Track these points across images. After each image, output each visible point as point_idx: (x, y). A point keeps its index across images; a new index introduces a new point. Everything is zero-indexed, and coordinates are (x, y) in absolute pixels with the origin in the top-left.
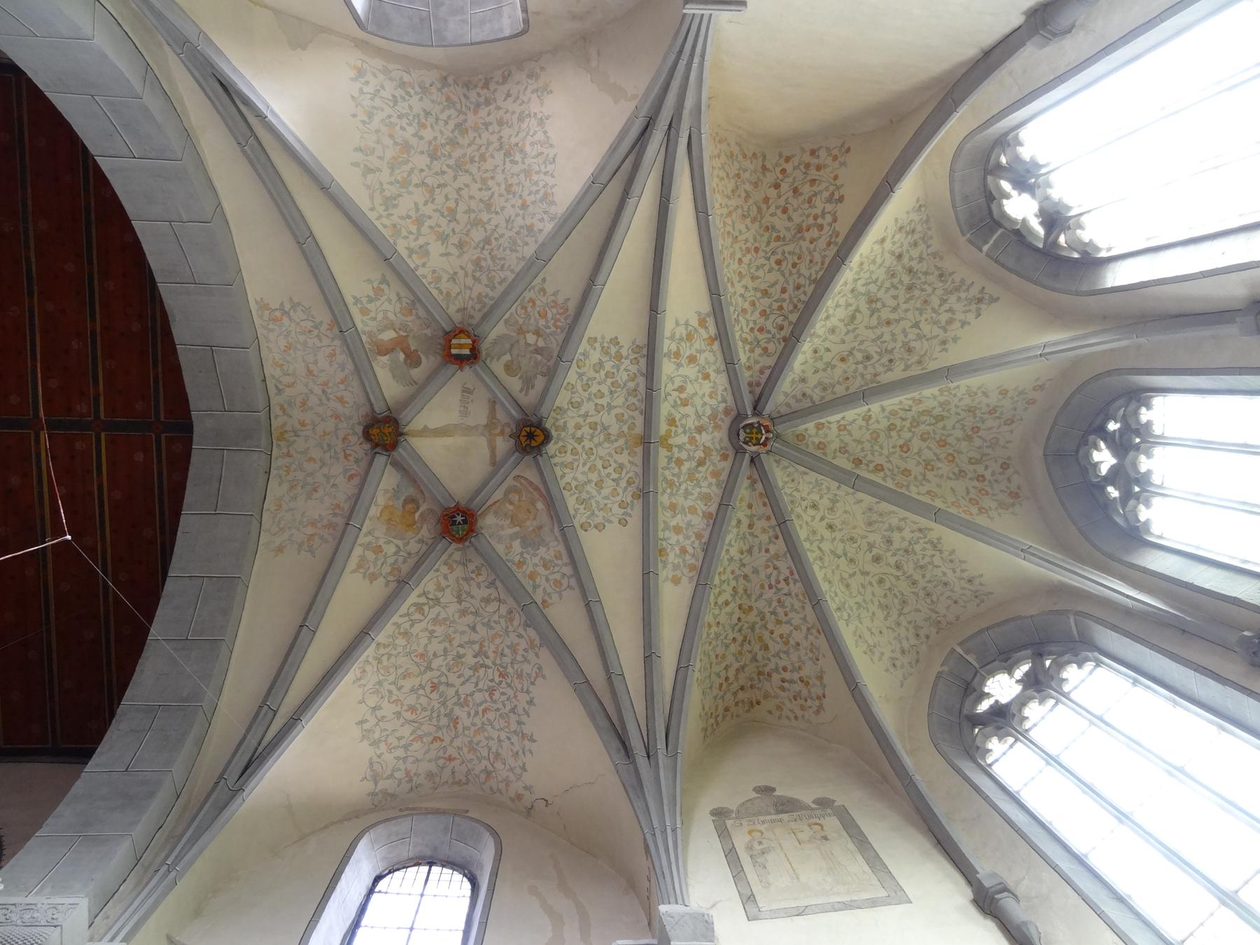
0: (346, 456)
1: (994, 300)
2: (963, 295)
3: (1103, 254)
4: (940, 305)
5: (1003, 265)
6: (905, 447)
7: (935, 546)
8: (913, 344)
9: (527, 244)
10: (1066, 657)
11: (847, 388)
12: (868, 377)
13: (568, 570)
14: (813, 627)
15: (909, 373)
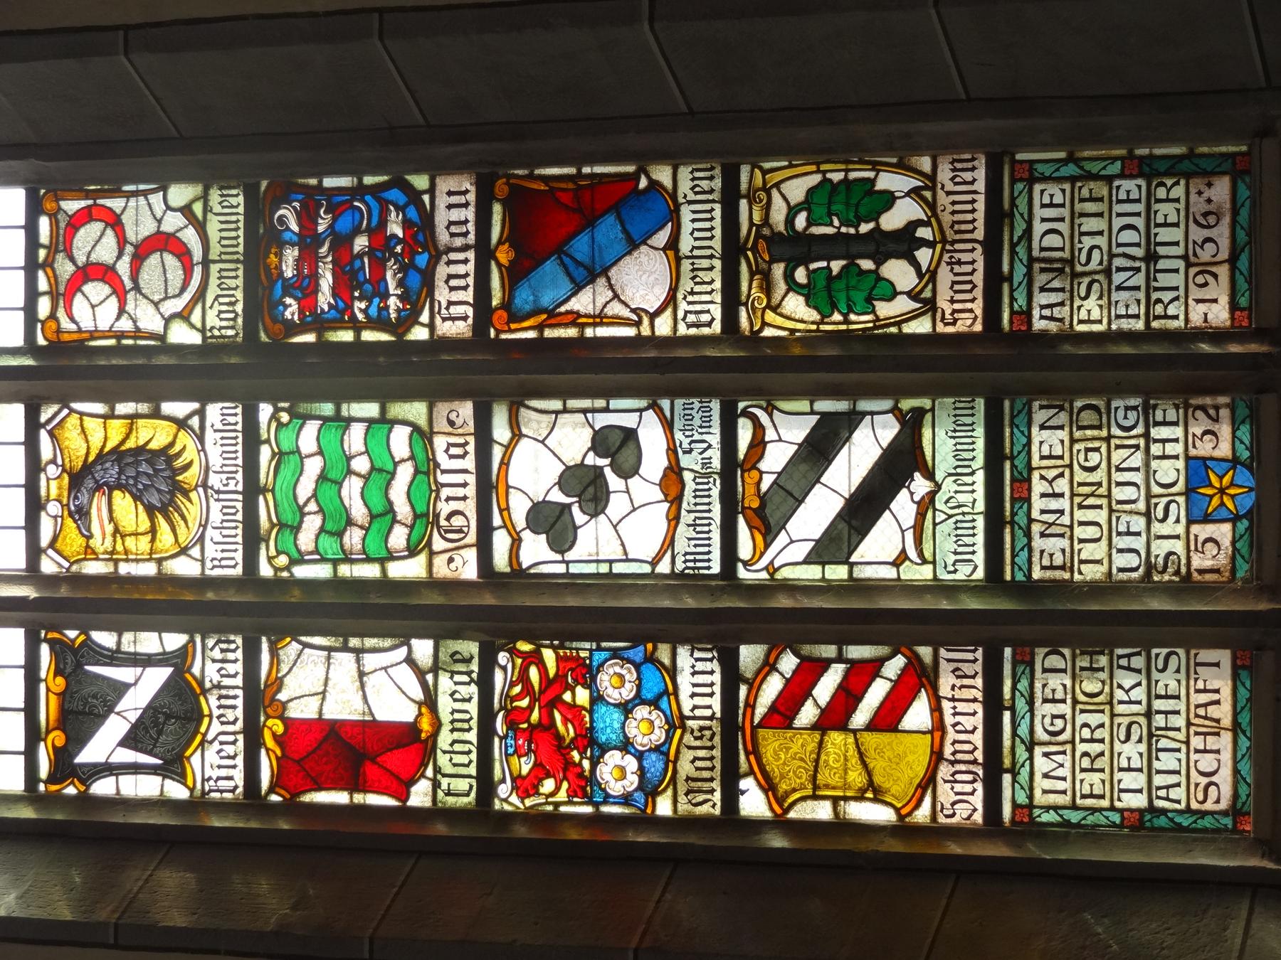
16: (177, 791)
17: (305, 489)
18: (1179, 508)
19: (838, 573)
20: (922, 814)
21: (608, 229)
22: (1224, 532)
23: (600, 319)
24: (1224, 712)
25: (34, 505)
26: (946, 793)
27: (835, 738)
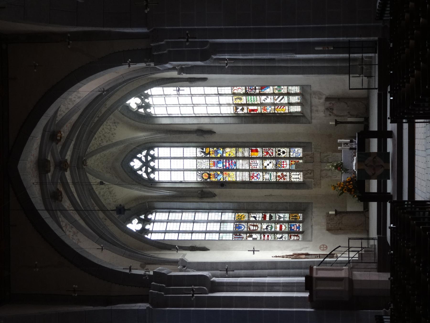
1: (118, 123)
2: (111, 121)
3: (154, 116)
4: (107, 124)
5: (123, 114)
6: (98, 165)
7: (110, 193)
8: (105, 135)
9: (69, 104)
10: (148, 213)
11: (94, 148)
12: (98, 144)
15: (108, 143)
16: (243, 112)
17: (249, 99)
18: (297, 99)
19: (280, 102)
20: (285, 112)
21: (266, 88)
22: (300, 100)
23: (266, 92)
24: (300, 107)
25: (233, 100)
26: (286, 111)
27: (280, 109)
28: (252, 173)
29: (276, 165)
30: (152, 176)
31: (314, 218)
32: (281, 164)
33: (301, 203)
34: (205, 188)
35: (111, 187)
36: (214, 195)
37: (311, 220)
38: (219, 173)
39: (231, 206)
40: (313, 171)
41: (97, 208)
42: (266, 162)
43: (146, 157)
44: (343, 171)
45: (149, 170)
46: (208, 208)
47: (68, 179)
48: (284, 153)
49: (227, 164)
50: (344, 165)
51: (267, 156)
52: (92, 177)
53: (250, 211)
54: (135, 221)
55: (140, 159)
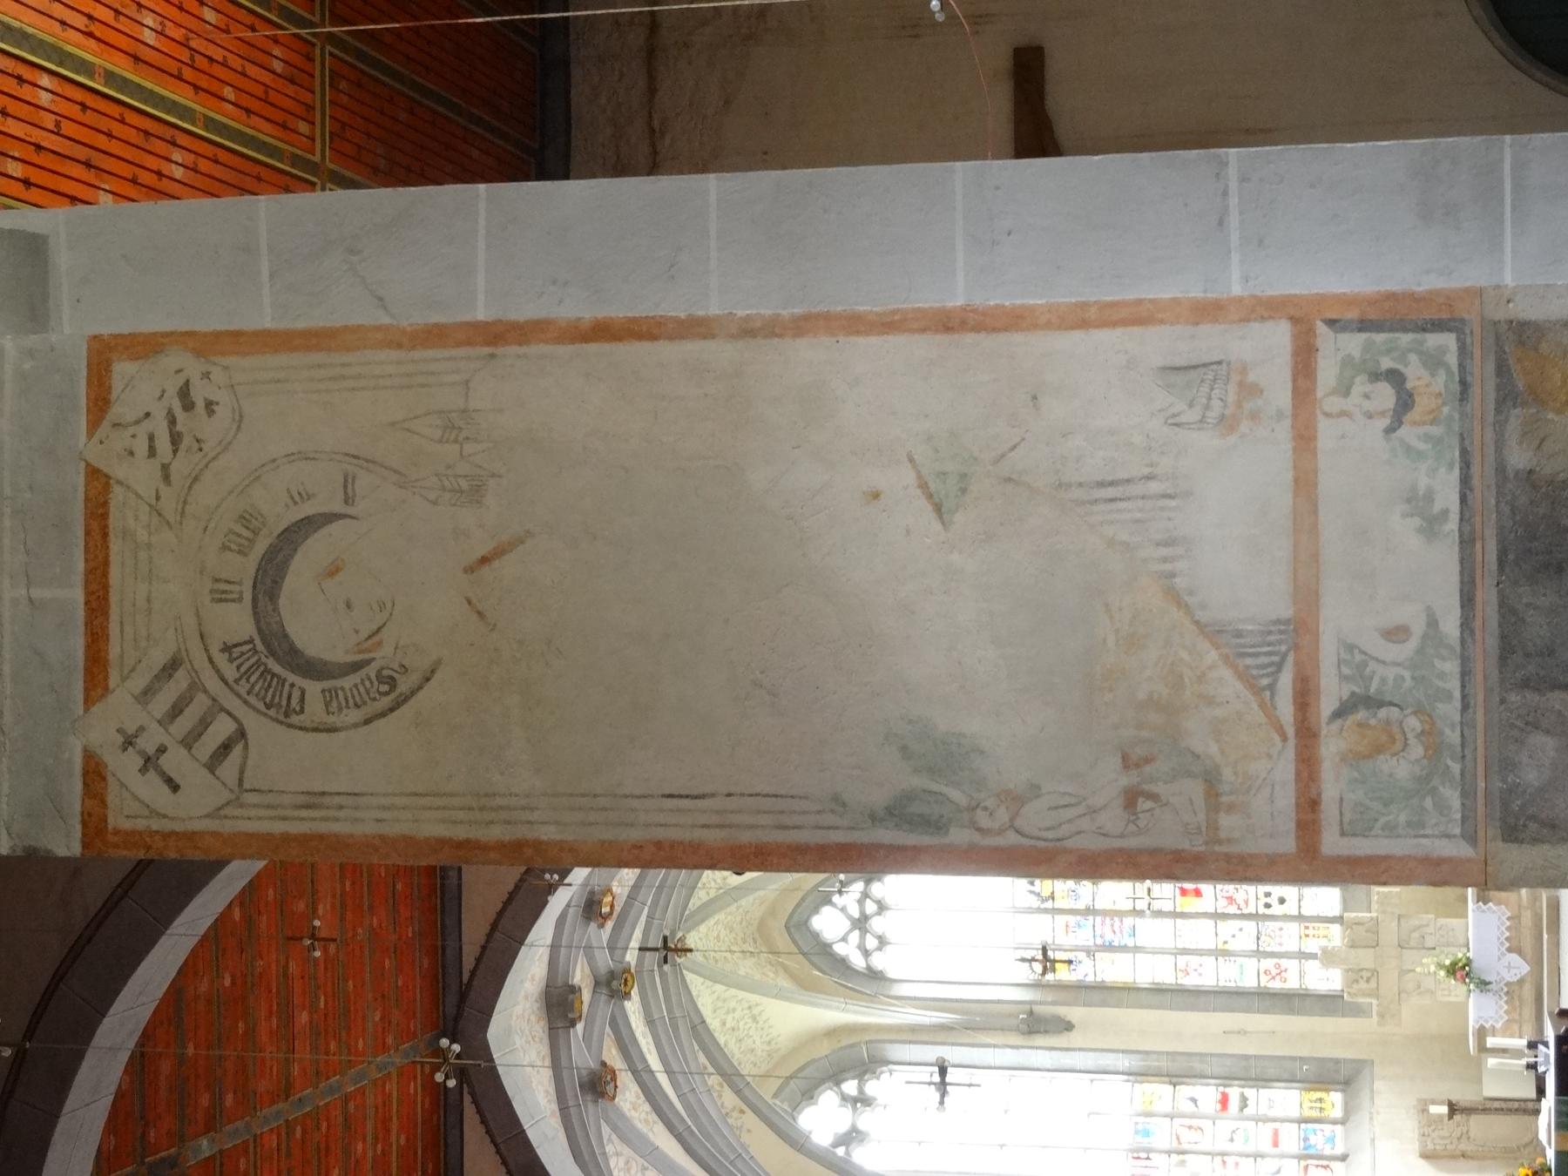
0: (533, 1038)
7: (754, 1019)
11: (708, 893)
12: (719, 881)
13: (647, 1107)
14: (734, 1109)
28: (1182, 960)
29: (1258, 939)
30: (879, 961)
31: (1378, 1113)
32: (1272, 934)
33: (1337, 1061)
34: (1041, 1003)
35: (757, 1005)
36: (1068, 1027)
37: (1371, 1119)
38: (1082, 956)
39: (1124, 1062)
40: (1375, 972)
41: (711, 1070)
42: (1227, 927)
43: (861, 902)
44: (1472, 986)
45: (871, 943)
46: (1049, 1066)
47: (634, 1013)
48: (1282, 901)
49: (1107, 930)
50: (1475, 965)
51: (1232, 910)
52: (702, 980)
53: (1180, 1080)
54: (828, 1098)
55: (843, 910)
